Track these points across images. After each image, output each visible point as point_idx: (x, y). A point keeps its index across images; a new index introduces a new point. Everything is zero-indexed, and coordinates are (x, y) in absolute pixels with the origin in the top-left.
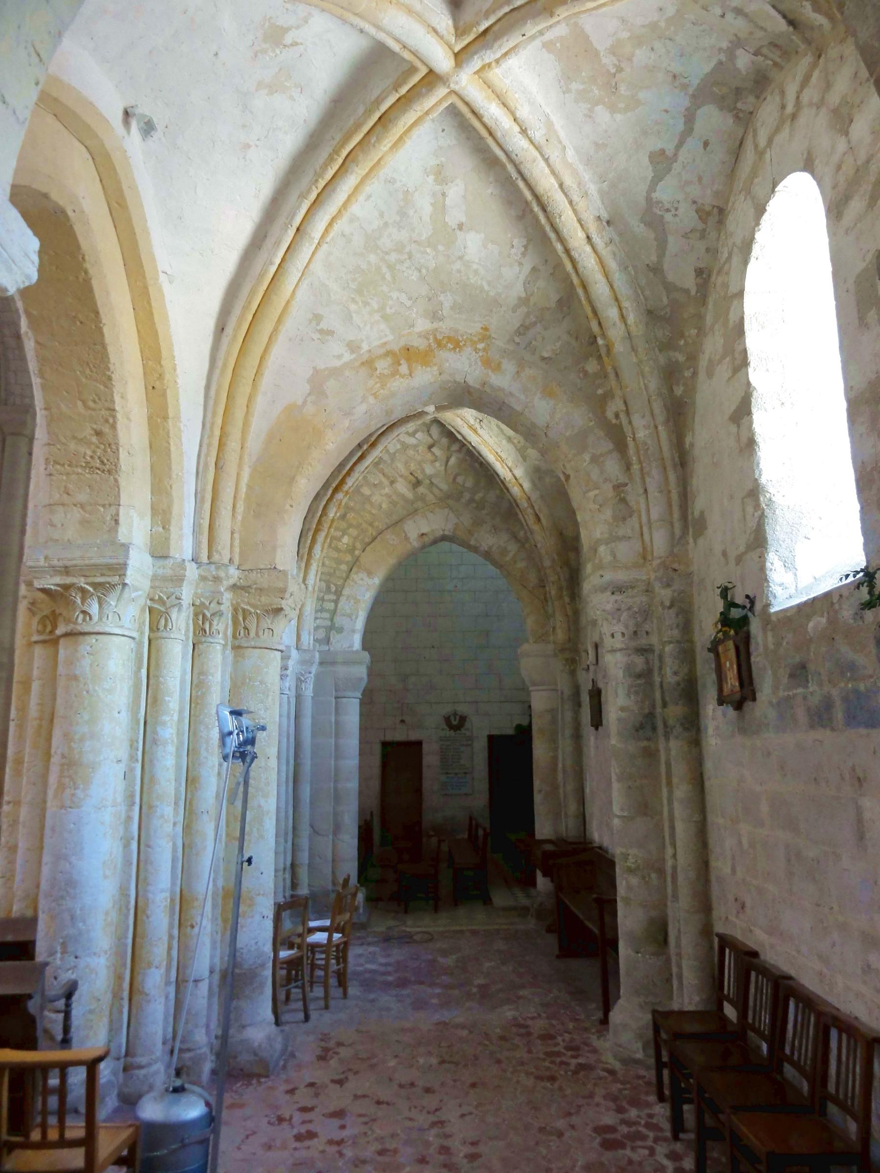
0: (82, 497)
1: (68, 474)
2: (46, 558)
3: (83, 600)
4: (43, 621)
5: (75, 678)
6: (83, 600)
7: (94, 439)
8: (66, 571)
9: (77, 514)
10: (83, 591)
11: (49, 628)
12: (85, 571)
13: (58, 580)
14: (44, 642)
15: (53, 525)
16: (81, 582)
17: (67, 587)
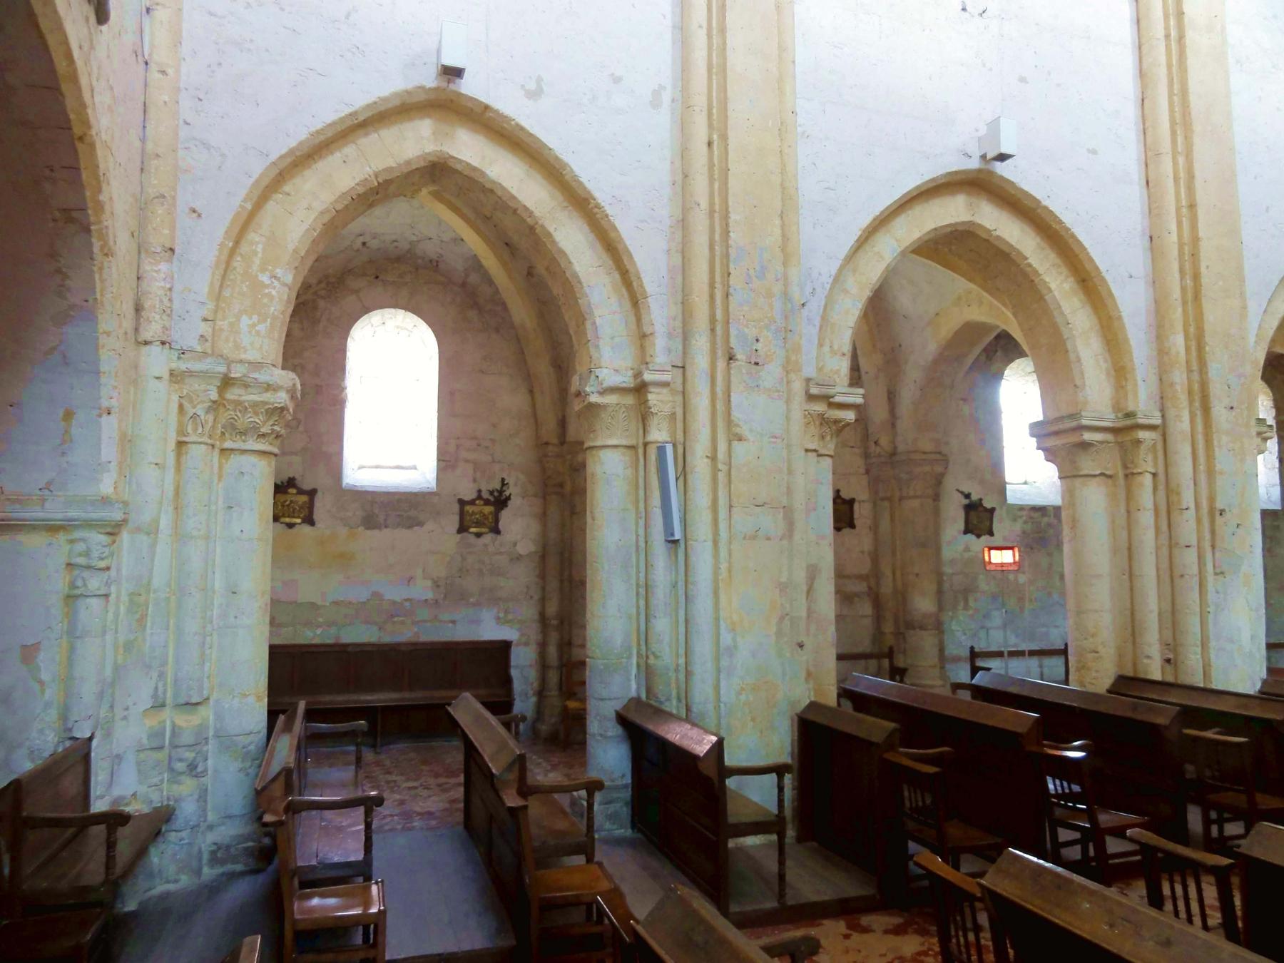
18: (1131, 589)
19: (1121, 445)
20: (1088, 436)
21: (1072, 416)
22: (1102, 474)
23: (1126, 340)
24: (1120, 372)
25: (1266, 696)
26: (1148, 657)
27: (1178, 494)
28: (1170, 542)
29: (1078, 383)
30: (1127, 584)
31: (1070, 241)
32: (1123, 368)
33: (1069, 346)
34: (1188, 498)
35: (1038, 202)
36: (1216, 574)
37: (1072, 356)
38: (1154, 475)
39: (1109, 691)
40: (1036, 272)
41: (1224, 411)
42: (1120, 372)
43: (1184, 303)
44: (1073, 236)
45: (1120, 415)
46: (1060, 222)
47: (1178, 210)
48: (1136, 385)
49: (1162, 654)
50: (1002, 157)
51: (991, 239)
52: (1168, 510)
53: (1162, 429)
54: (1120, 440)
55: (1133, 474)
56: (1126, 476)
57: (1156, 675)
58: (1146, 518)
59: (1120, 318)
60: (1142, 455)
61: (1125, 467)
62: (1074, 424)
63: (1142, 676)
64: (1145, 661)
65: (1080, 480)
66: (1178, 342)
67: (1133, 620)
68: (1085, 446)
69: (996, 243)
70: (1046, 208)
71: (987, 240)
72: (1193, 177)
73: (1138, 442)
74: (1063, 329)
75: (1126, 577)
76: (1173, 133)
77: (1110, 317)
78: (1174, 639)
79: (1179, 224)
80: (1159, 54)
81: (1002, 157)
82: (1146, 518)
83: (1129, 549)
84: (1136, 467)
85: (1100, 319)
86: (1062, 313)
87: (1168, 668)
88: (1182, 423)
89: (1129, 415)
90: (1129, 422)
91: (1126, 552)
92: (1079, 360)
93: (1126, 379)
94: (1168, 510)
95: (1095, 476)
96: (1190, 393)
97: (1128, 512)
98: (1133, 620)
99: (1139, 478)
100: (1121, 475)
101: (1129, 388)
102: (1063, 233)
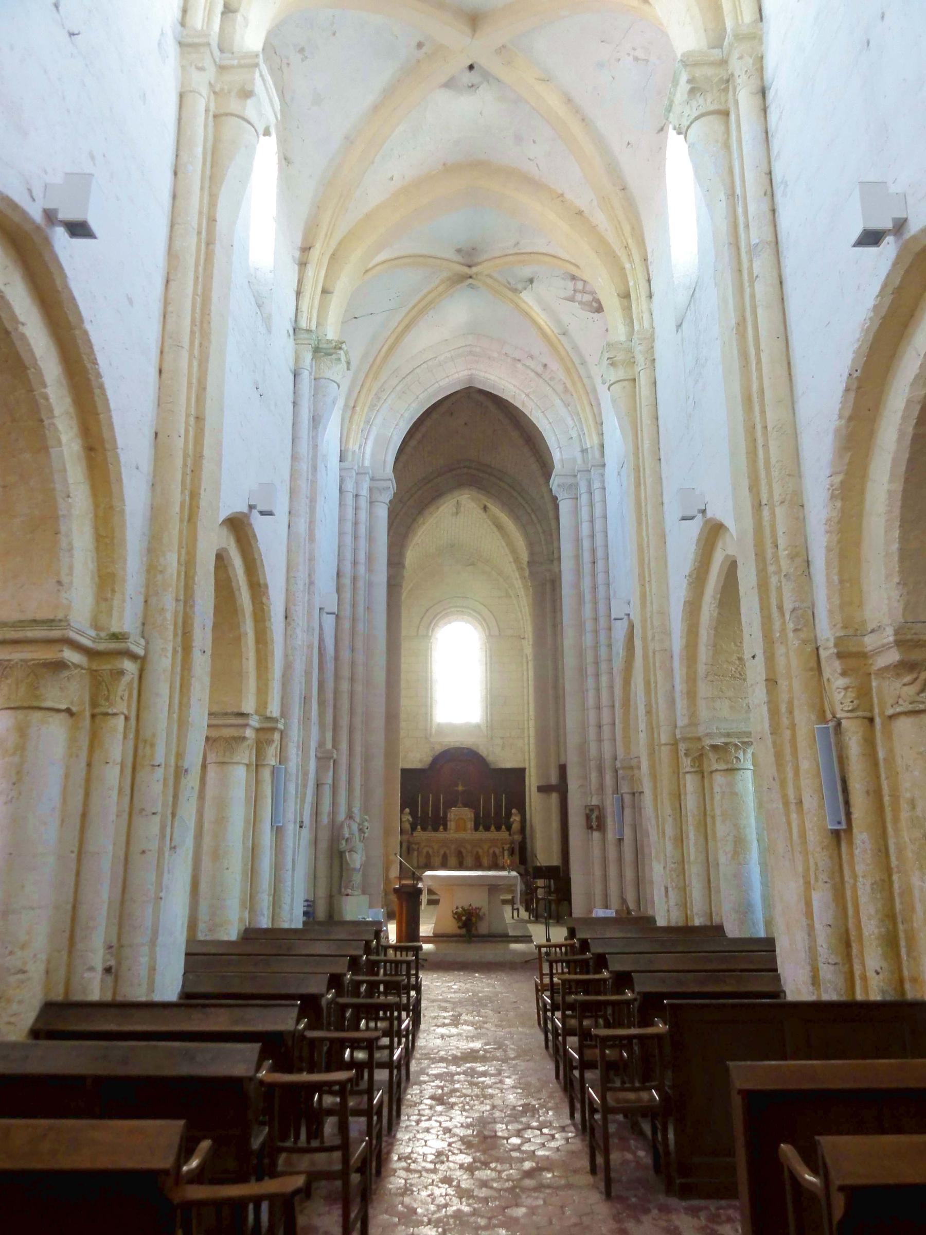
0: (730, 693)
1: (722, 681)
2: (717, 728)
3: (736, 751)
4: (693, 760)
5: (736, 794)
6: (736, 751)
7: (737, 662)
8: (728, 735)
9: (727, 702)
10: (736, 745)
11: (697, 765)
12: (738, 735)
13: (723, 740)
14: (695, 772)
15: (715, 709)
16: (736, 741)
17: (726, 744)
18: (78, 874)
19: (93, 673)
20: (70, 655)
21: (49, 623)
22: (68, 711)
23: (123, 541)
24: (106, 581)
25: (191, 999)
26: (91, 969)
27: (152, 745)
28: (133, 810)
29: (65, 579)
30: (73, 866)
31: (97, 391)
32: (113, 576)
33: (63, 529)
34: (160, 754)
35: (80, 319)
36: (171, 848)
37: (64, 544)
38: (127, 718)
39: (36, 1033)
40: (50, 410)
41: (199, 653)
42: (106, 581)
43: (181, 521)
44: (102, 387)
45: (103, 634)
46: (95, 362)
47: (188, 416)
48: (124, 601)
49: (104, 961)
50: (79, 229)
51: (14, 335)
52: (135, 766)
53: (142, 661)
54: (94, 667)
55: (106, 714)
56: (93, 716)
57: (95, 994)
58: (112, 777)
59: (122, 512)
60: (120, 693)
61: (94, 704)
62: (56, 634)
63: (77, 997)
64: (87, 975)
65: (38, 715)
66: (172, 561)
67: (74, 919)
68: (60, 666)
69: (18, 344)
70: (86, 333)
71: (7, 333)
72: (205, 389)
73: (121, 673)
74: (60, 500)
75: (74, 856)
76: (192, 333)
77: (111, 507)
78: (119, 939)
79: (187, 431)
80: (190, 244)
81: (79, 229)
82: (112, 777)
83: (84, 815)
84: (111, 705)
85: (96, 506)
86: (65, 480)
87: (110, 979)
88: (164, 662)
89: (115, 637)
90: (113, 646)
91: (77, 821)
92: (71, 549)
93: (113, 591)
94: (135, 766)
95: (58, 711)
96: (175, 624)
97: (89, 765)
98: (74, 919)
99: (112, 721)
100: (88, 714)
101: (116, 603)
102: (92, 377)
